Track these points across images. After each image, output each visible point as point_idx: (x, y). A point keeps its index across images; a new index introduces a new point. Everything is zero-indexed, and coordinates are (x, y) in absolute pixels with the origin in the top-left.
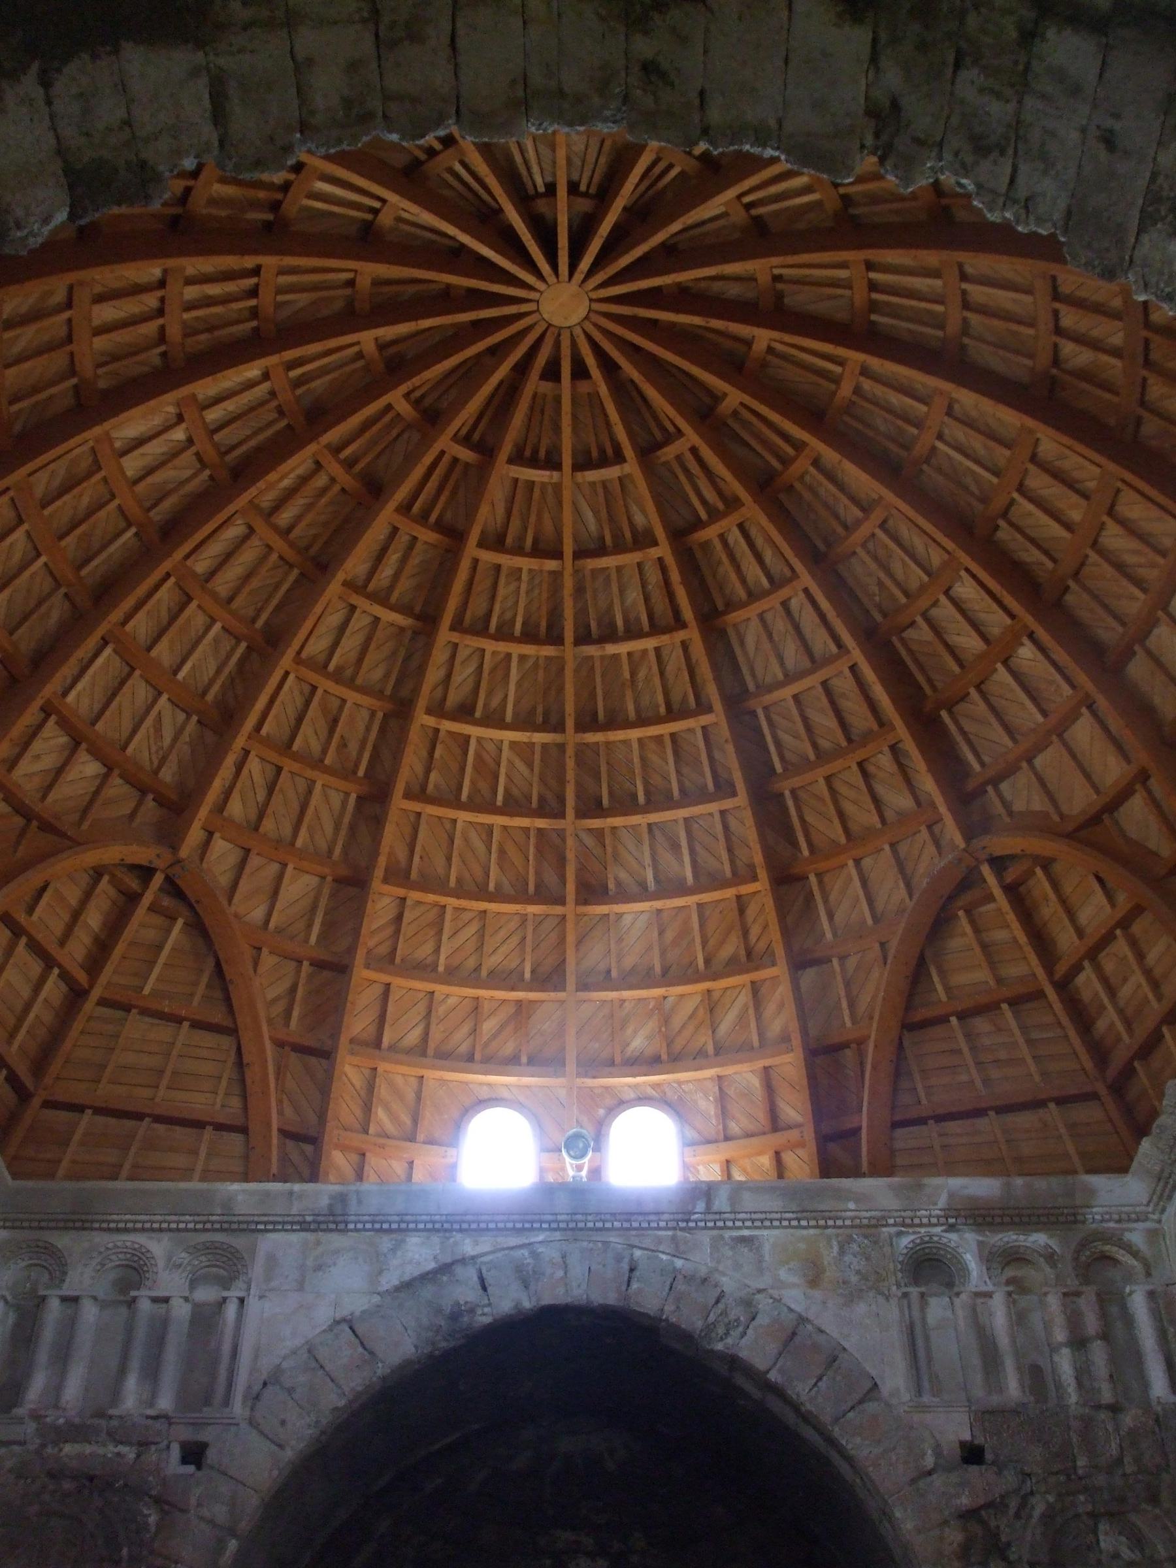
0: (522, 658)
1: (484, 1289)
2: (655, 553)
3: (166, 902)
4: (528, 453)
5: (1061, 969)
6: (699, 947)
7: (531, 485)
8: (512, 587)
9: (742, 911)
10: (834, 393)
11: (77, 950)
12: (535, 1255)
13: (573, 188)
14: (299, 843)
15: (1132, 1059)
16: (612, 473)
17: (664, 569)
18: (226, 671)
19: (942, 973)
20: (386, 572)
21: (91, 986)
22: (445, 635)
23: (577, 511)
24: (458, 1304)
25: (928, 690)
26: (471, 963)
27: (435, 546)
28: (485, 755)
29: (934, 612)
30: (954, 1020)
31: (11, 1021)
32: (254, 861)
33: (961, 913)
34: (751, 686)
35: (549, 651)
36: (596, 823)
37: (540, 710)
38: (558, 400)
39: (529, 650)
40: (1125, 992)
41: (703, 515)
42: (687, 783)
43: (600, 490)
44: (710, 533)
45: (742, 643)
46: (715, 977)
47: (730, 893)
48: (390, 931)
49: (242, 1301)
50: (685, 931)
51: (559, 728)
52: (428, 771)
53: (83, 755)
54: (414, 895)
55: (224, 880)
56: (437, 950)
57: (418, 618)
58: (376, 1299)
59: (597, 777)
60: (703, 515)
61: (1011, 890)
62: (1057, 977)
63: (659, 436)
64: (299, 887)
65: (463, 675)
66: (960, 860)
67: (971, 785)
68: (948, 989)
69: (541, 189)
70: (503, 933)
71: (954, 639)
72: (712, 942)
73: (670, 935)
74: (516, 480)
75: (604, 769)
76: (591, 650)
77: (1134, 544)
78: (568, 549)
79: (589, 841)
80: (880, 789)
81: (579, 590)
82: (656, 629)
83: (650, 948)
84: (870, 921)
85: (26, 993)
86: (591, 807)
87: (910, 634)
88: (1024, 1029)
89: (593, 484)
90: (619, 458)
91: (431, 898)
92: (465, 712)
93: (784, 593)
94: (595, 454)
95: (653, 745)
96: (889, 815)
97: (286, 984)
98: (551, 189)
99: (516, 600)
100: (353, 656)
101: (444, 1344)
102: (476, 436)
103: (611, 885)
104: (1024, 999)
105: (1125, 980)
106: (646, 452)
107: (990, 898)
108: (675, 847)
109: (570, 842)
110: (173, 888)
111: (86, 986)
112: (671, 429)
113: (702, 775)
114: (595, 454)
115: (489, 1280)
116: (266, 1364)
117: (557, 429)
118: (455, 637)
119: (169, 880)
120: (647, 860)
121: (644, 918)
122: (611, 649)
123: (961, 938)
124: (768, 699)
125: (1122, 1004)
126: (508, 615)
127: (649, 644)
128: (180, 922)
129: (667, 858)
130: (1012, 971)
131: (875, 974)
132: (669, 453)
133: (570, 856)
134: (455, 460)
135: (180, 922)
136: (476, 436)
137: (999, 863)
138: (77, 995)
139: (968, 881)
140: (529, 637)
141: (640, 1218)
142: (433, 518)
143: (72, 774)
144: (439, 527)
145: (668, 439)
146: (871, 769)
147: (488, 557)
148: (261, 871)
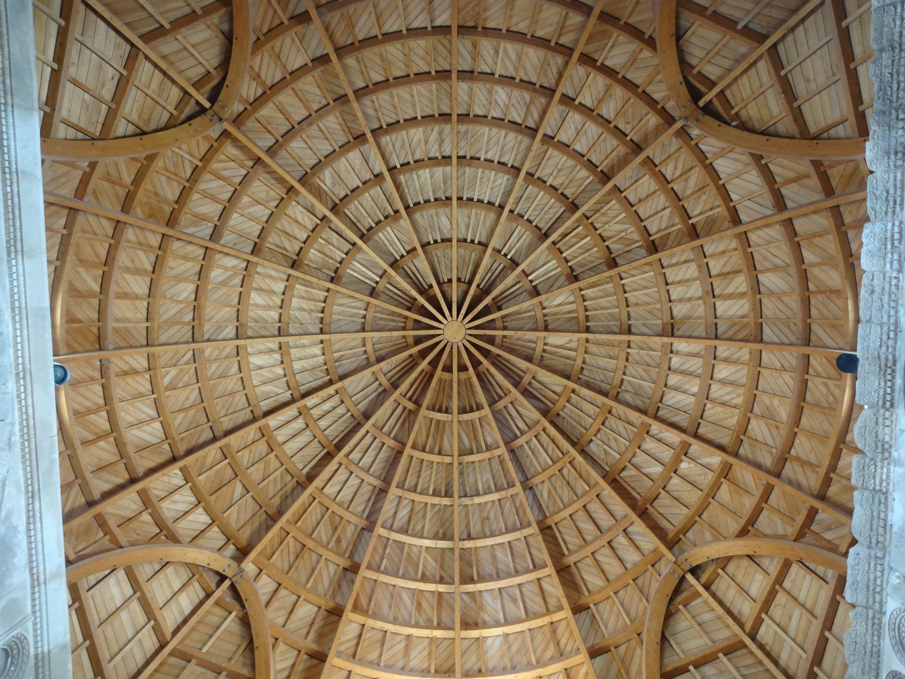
0: (434, 505)
2: (497, 452)
3: (229, 599)
4: (437, 407)
5: (748, 627)
6: (532, 653)
7: (438, 421)
8: (429, 472)
9: (554, 632)
10: (573, 366)
11: (169, 625)
13: (459, 280)
14: (309, 586)
15: (811, 668)
16: (475, 415)
17: (502, 462)
18: (285, 490)
19: (677, 644)
20: (367, 460)
21: (172, 639)
22: (394, 491)
23: (459, 436)
25: (638, 497)
26: (400, 664)
27: (393, 449)
28: (412, 554)
29: (634, 460)
31: (116, 649)
32: (283, 592)
33: (681, 607)
34: (548, 514)
35: (446, 501)
36: (470, 588)
37: (441, 531)
38: (452, 380)
39: (436, 500)
40: (793, 626)
41: (518, 433)
42: (519, 567)
43: (470, 423)
44: (521, 441)
45: (542, 495)
46: (544, 666)
47: (546, 620)
48: (354, 642)
50: (524, 644)
51: (451, 539)
52: (382, 559)
53: (200, 510)
54: (370, 622)
55: (264, 599)
56: (381, 656)
57: (383, 481)
59: (471, 566)
60: (518, 433)
61: (707, 587)
62: (747, 630)
63: (496, 398)
64: (306, 611)
65: (403, 513)
66: (674, 572)
67: (670, 536)
68: (683, 652)
69: (446, 280)
70: (418, 649)
71: (647, 470)
72: (539, 652)
73: (514, 649)
74: (432, 419)
75: (474, 563)
76: (466, 501)
77: (728, 389)
78: (456, 454)
79: (467, 599)
80: (620, 553)
81: (461, 474)
82: (498, 489)
83: (503, 656)
84: (628, 622)
85: (130, 634)
86: (467, 579)
87: (624, 474)
88: (737, 668)
89: (467, 422)
90: (479, 407)
91: (379, 624)
92: (404, 531)
93: (559, 465)
94: (468, 408)
95: (498, 549)
96: (629, 566)
97: (290, 662)
98: (450, 281)
99: (430, 479)
100: (349, 498)
102: (414, 398)
103: (480, 621)
104: (730, 650)
105: (790, 618)
106: (492, 403)
107: (697, 595)
108: (514, 601)
109: (457, 598)
110: (233, 587)
111: (169, 639)
112: (502, 394)
113: (526, 562)
114: (468, 408)
117: (450, 397)
118: (399, 492)
120: (499, 607)
121: (498, 641)
122: (477, 500)
123: (683, 623)
124: (557, 518)
125: (792, 635)
126: (426, 486)
127: (495, 496)
129: (509, 606)
131: (638, 651)
132: (500, 405)
133: (457, 607)
134: (405, 408)
135: (234, 614)
136: (414, 398)
137: (695, 571)
138: (162, 647)
139: (680, 586)
140: (436, 494)
142: (392, 435)
143: (191, 517)
144: (395, 439)
145: (501, 398)
146: (615, 545)
147: (417, 454)
148: (285, 598)
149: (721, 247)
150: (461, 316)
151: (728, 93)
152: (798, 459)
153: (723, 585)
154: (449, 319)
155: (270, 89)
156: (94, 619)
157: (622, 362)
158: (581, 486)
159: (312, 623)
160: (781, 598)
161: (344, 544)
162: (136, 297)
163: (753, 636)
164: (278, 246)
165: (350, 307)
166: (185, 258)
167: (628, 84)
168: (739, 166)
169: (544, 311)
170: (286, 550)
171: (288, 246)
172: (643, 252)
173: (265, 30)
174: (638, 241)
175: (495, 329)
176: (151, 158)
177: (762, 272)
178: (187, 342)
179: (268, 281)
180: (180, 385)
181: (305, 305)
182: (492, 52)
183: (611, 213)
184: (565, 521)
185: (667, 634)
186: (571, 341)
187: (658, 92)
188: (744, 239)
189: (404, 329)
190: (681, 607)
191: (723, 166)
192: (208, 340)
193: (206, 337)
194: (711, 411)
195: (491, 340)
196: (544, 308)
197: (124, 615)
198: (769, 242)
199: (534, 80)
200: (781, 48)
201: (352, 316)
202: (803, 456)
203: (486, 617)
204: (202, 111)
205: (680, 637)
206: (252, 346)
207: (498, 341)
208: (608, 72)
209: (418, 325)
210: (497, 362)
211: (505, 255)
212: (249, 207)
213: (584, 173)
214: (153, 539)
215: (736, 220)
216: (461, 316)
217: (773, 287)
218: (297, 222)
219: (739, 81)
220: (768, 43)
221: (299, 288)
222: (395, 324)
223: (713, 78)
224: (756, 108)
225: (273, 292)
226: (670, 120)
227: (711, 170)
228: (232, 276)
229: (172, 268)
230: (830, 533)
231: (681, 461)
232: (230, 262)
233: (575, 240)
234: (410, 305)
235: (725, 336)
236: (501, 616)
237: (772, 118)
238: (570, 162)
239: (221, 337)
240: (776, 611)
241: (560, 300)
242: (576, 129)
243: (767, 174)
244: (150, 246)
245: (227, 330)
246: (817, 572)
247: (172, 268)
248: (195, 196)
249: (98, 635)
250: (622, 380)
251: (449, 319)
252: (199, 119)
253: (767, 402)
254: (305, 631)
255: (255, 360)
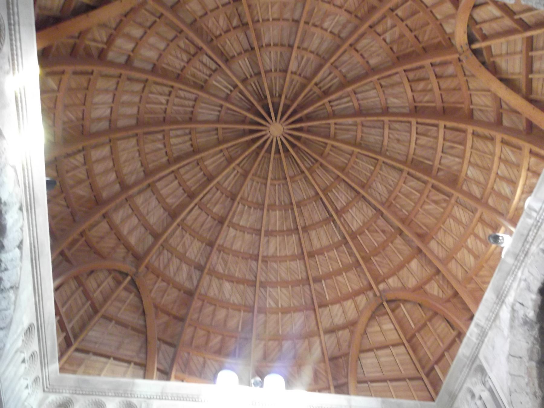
1: (523, 305)
12: (525, 280)
24: (522, 318)
30: (530, 76)
49: (489, 377)
58: (509, 340)
101: (534, 332)
108: (452, 148)
115: (521, 301)
116: (506, 389)
119: (388, 302)
120: (452, 158)
127: (387, 131)
128: (402, 305)
130: (519, 47)
141: (529, 237)
153: (486, 28)
156: (378, 375)
157: (318, 31)
158: (396, 78)
159: (422, 266)
161: (386, 229)
162: (227, 316)
163: (526, 27)
165: (251, 190)
166: (209, 286)
169: (273, 70)
171: (209, 225)
173: (88, 249)
175: (279, 104)
176: (156, 307)
179: (228, 238)
181: (245, 217)
184: (415, 97)
185: (504, 76)
190: (492, 60)
192: (256, 277)
193: (254, 278)
195: (287, 107)
196: (271, 70)
197: (382, 359)
201: (255, 189)
203: (455, 168)
204: (133, 282)
205: (510, 70)
206: (263, 252)
207: (288, 102)
209: (269, 151)
210: (302, 107)
211: (231, 91)
214: (352, 332)
221: (235, 220)
225: (235, 237)
229: (215, 294)
236: (457, 160)
239: (255, 270)
241: (269, 59)
245: (252, 265)
247: (215, 294)
248: (177, 279)
249: (388, 375)
250: (331, 32)
252: (137, 284)
254: (424, 270)
255: (271, 251)
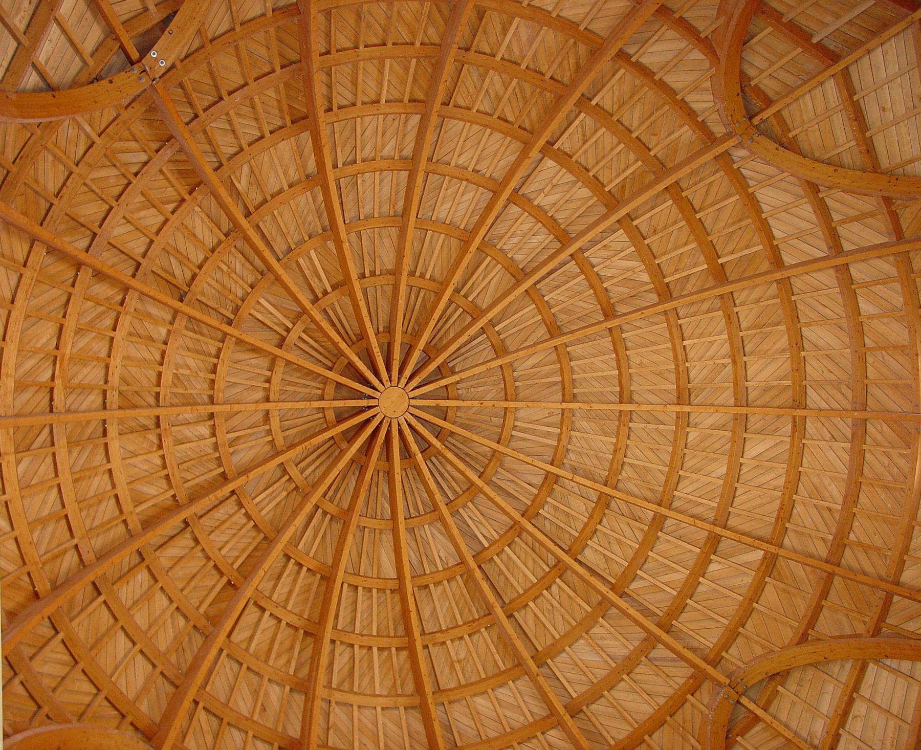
149: (756, 294)
150: (404, 381)
151: (785, 113)
152: (860, 544)
154: (388, 384)
155: (211, 41)
160: (859, 708)
164: (166, 271)
167: (662, 86)
168: (789, 198)
170: (198, 728)
171: (178, 272)
172: (654, 298)
174: (647, 284)
177: (809, 324)
178: (42, 413)
180: (34, 482)
182: (499, 27)
183: (619, 246)
186: (551, 415)
187: (702, 102)
188: (786, 286)
189: (322, 398)
191: (768, 197)
194: (744, 497)
198: (818, 291)
199: (544, 69)
200: (853, 70)
202: (866, 541)
208: (643, 70)
212: (139, 210)
213: (585, 192)
215: (778, 263)
216: (404, 381)
217: (821, 343)
218: (194, 235)
219: (801, 101)
220: (842, 65)
222: (308, 390)
223: (770, 94)
224: (818, 133)
226: (710, 139)
227: (752, 202)
228: (104, 313)
230: (911, 623)
231: (710, 561)
232: (102, 290)
233: (562, 279)
234: (330, 364)
235: (758, 403)
237: (836, 146)
238: (570, 178)
240: (855, 726)
242: (584, 135)
243: (823, 210)
244: (14, 261)
246: (902, 670)
251: (388, 384)
253: (816, 481)
